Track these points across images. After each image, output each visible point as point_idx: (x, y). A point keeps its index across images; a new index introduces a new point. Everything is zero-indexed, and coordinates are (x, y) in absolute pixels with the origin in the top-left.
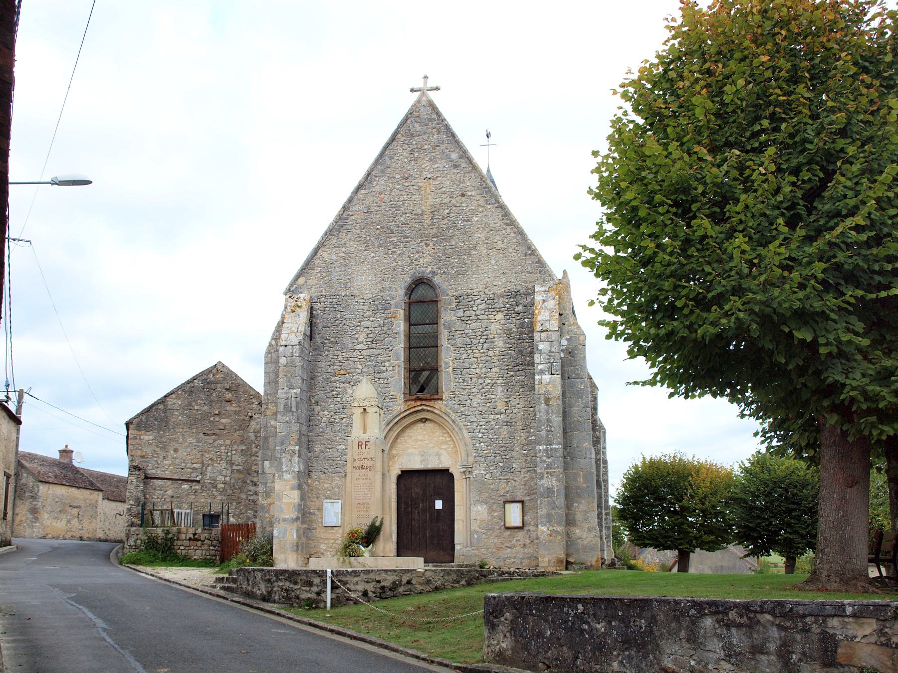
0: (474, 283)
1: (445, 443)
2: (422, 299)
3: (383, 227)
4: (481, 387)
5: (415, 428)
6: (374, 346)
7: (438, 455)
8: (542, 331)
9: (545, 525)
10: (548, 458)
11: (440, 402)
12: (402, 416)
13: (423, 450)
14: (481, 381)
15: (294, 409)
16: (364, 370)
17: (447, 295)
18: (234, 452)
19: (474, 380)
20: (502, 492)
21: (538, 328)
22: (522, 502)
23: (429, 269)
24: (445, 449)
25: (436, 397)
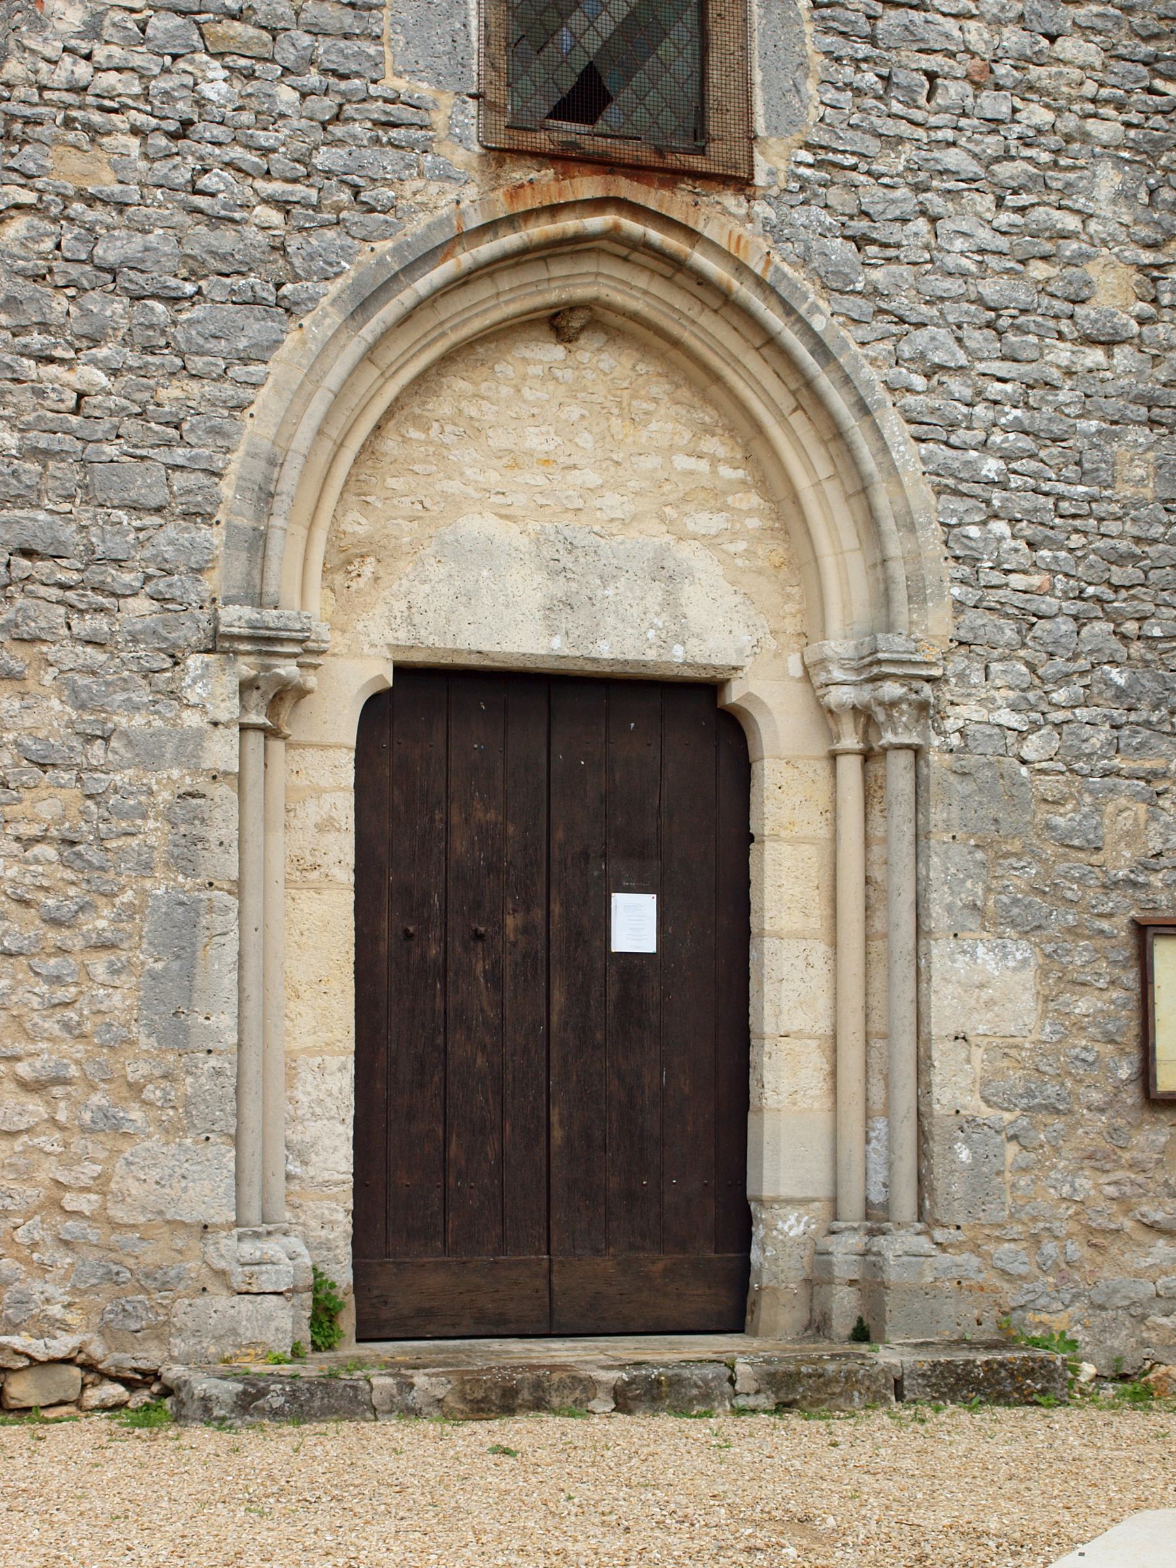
1: (715, 497)
4: (992, 144)
5: (505, 369)
7: (666, 574)
11: (731, 201)
12: (465, 258)
13: (564, 525)
14: (995, 104)
19: (953, 91)
20: (1121, 861)
22: (1144, 933)
24: (711, 542)
25: (697, 163)
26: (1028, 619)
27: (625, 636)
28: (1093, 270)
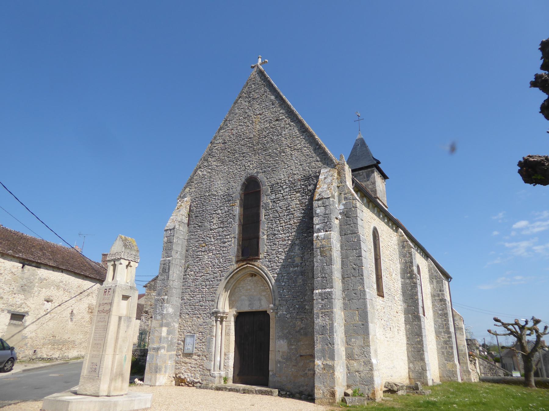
0: (282, 175)
2: (251, 191)
3: (231, 150)
6: (222, 226)
8: (318, 200)
9: (320, 359)
10: (322, 300)
16: (216, 242)
17: (266, 185)
21: (317, 197)
23: (256, 170)
26: (287, 301)
27: (256, 307)
28: (295, 259)
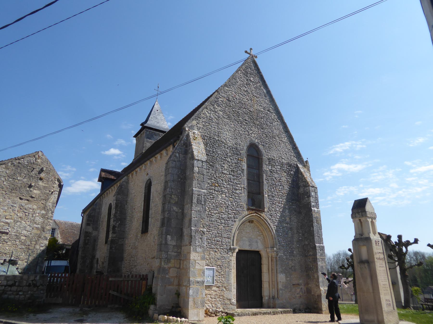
0: (274, 154)
3: (235, 111)
15: (203, 203)
18: (37, 214)
23: (257, 141)
24: (260, 239)
26: (283, 246)
27: (254, 248)
